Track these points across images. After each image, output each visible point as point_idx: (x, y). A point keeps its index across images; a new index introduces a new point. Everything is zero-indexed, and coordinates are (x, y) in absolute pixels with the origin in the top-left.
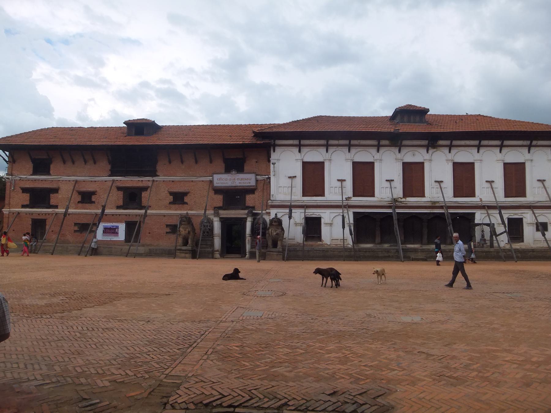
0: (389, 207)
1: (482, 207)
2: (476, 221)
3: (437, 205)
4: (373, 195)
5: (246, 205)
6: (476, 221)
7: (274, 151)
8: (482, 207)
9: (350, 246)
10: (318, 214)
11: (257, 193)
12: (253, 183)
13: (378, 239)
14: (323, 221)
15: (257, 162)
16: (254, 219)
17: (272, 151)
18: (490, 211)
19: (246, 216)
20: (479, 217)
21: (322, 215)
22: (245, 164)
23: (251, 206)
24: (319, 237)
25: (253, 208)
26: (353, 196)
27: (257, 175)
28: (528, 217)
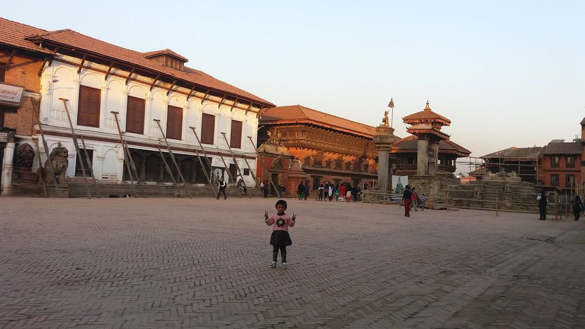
0: (156, 146)
1: (218, 154)
2: (212, 165)
3: (189, 148)
4: (142, 133)
5: (5, 126)
6: (213, 165)
7: (50, 65)
8: (218, 154)
9: (119, 182)
10: (91, 146)
11: (20, 112)
12: (17, 99)
13: (143, 177)
14: (95, 154)
15: (24, 73)
16: (16, 145)
17: (47, 64)
18: (224, 158)
19: (5, 141)
20: (216, 162)
21: (95, 148)
22: (6, 73)
23: (11, 128)
24: (89, 173)
25: (14, 130)
26: (126, 131)
27: (26, 90)
28: (241, 164)
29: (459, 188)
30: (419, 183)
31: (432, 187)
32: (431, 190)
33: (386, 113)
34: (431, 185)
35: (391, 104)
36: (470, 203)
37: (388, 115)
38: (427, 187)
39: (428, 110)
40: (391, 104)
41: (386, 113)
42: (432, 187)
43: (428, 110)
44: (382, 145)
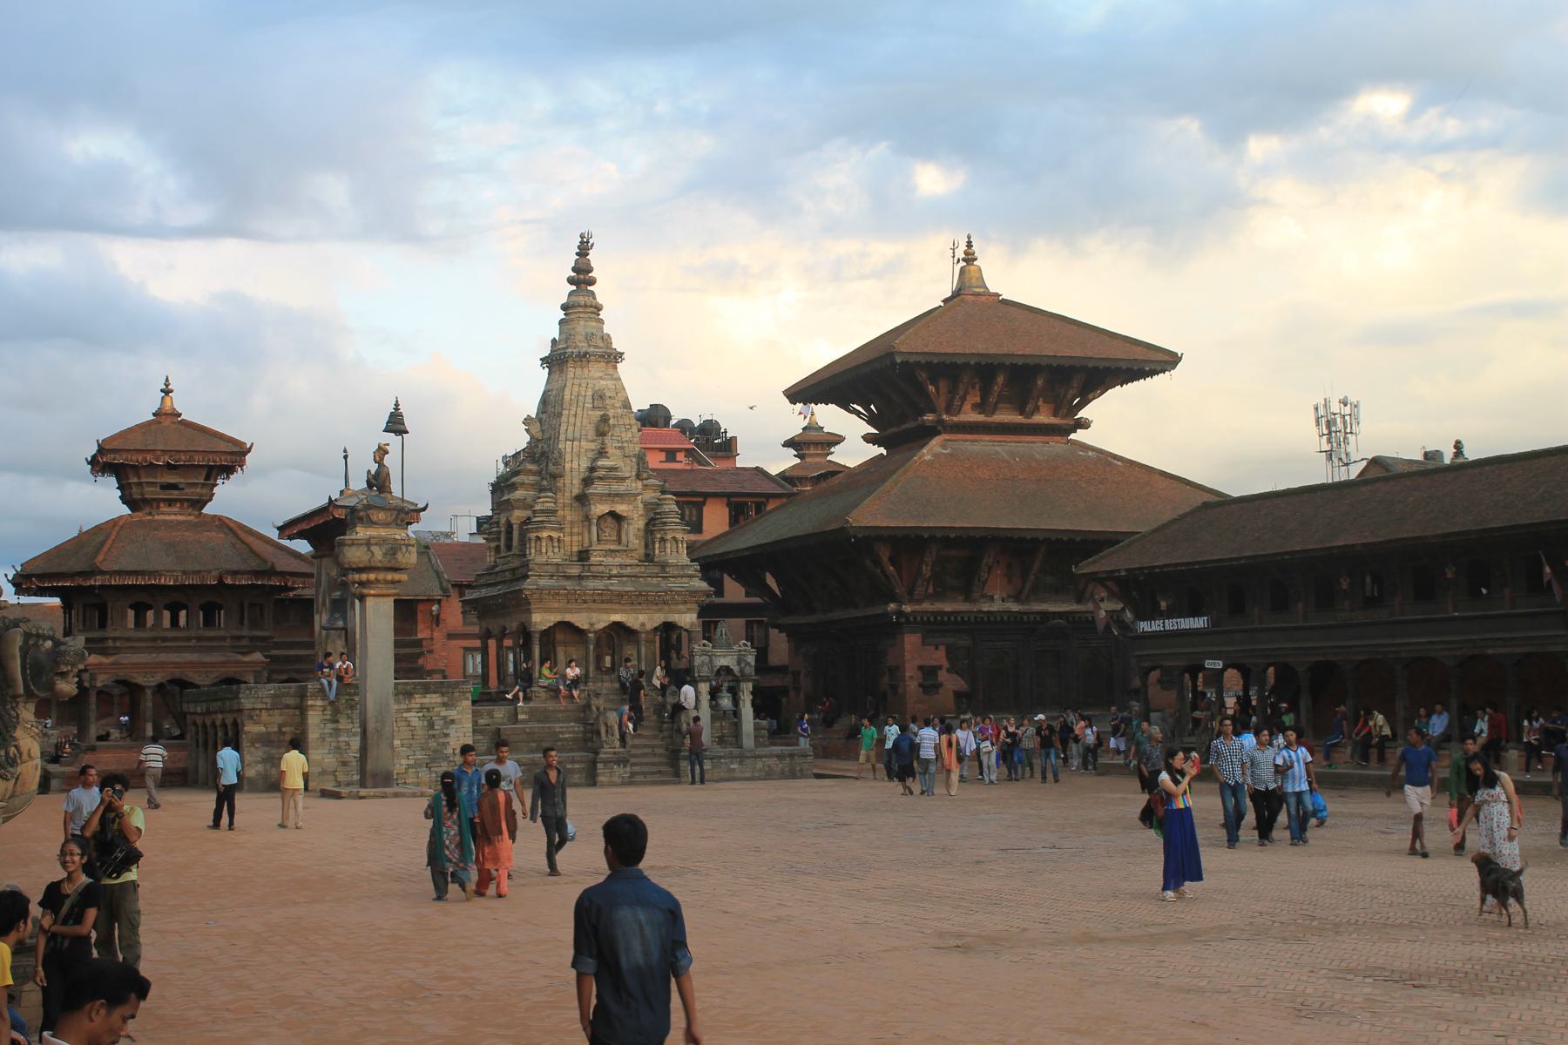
29: (521, 717)
30: (409, 710)
31: (453, 721)
32: (452, 730)
33: (382, 451)
34: (452, 714)
35: (396, 424)
36: (600, 766)
37: (387, 460)
38: (438, 724)
39: (166, 416)
40: (396, 424)
41: (382, 451)
42: (453, 721)
43: (166, 416)
44: (390, 576)
